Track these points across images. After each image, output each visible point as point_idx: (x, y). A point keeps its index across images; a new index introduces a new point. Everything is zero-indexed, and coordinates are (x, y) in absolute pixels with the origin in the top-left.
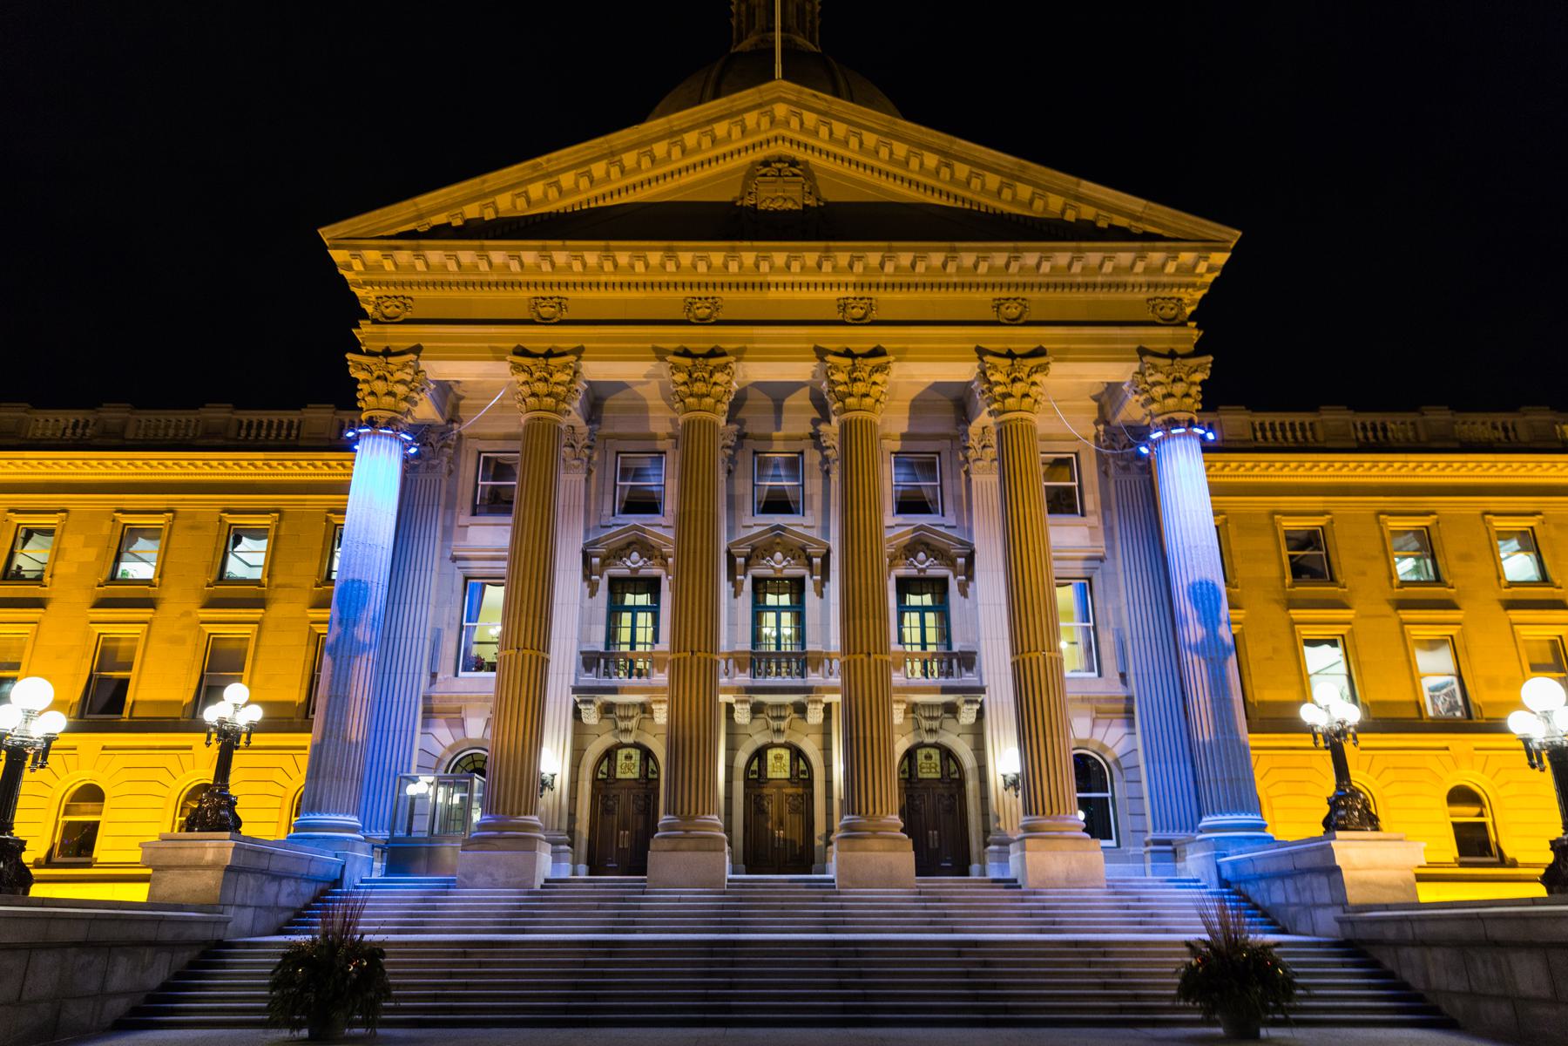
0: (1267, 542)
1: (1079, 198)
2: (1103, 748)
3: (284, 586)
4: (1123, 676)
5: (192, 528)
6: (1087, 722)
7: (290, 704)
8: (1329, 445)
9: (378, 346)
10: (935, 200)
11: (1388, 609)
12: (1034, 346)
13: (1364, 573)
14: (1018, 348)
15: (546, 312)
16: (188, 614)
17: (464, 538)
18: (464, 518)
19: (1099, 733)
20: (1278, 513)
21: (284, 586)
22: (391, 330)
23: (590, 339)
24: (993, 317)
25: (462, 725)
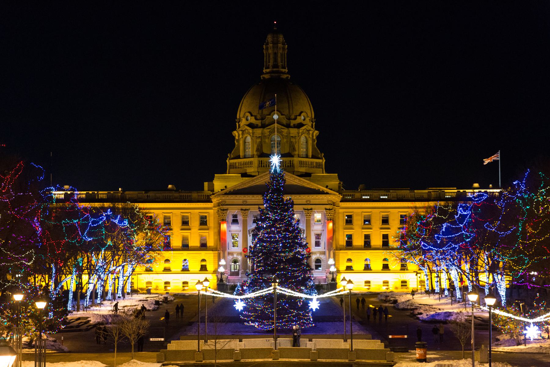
0: (360, 218)
1: (318, 187)
2: (321, 258)
3: (194, 226)
4: (325, 248)
5: (176, 216)
6: (319, 254)
7: (198, 246)
8: (374, 199)
9: (222, 209)
10: (299, 184)
11: (379, 229)
12: (310, 208)
13: (376, 223)
14: (309, 208)
15: (245, 203)
16: (178, 231)
17: (230, 228)
18: (230, 225)
19: (320, 256)
20: (363, 212)
21: (194, 226)
22: (224, 206)
23: (251, 207)
24: (305, 203)
25: (233, 255)
